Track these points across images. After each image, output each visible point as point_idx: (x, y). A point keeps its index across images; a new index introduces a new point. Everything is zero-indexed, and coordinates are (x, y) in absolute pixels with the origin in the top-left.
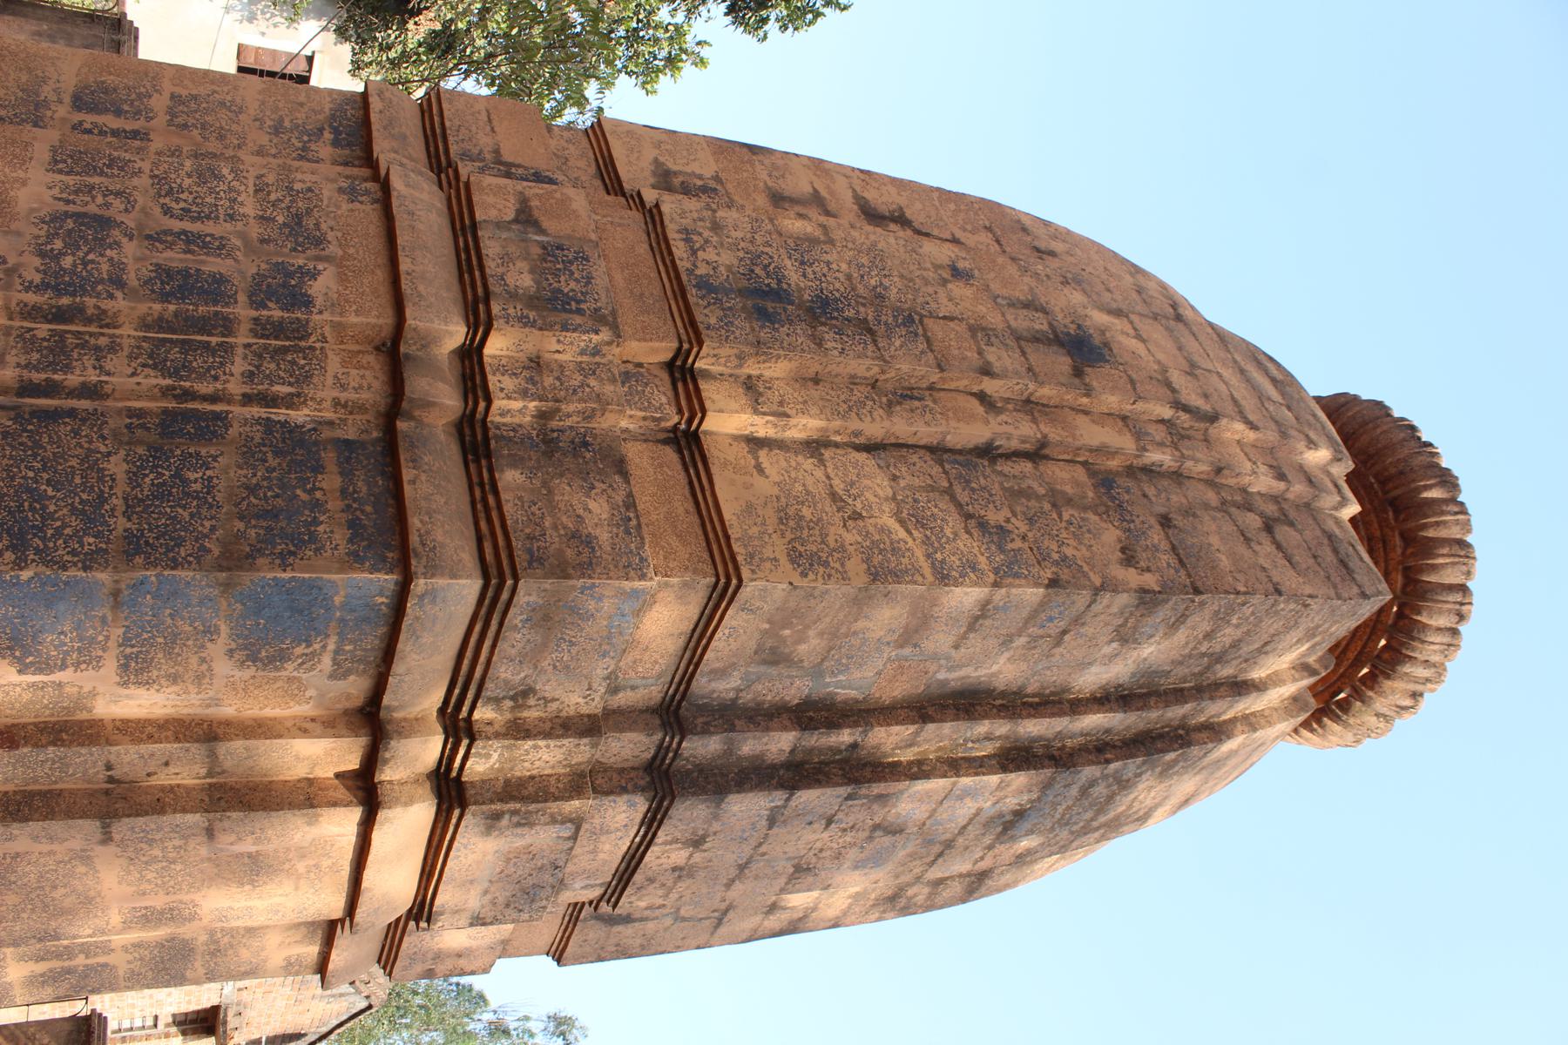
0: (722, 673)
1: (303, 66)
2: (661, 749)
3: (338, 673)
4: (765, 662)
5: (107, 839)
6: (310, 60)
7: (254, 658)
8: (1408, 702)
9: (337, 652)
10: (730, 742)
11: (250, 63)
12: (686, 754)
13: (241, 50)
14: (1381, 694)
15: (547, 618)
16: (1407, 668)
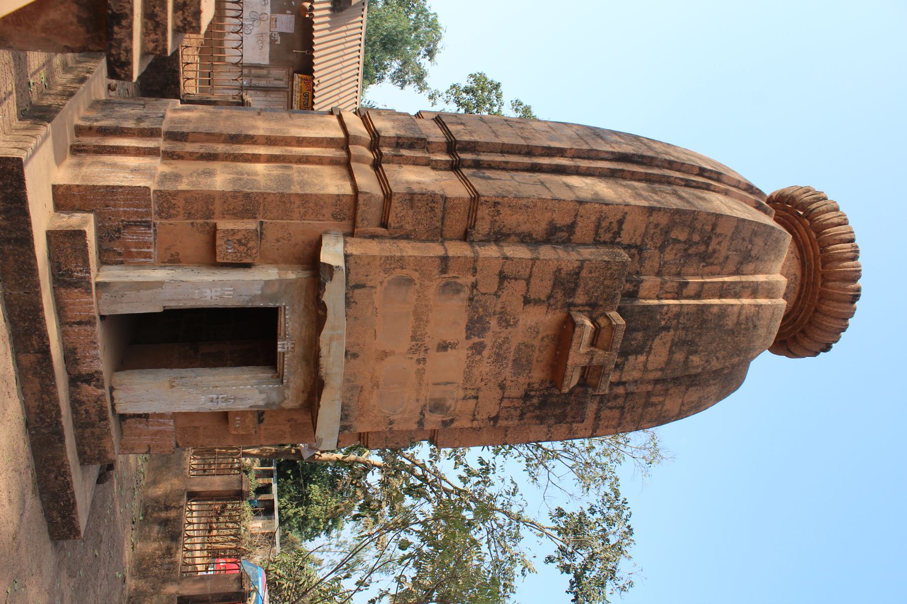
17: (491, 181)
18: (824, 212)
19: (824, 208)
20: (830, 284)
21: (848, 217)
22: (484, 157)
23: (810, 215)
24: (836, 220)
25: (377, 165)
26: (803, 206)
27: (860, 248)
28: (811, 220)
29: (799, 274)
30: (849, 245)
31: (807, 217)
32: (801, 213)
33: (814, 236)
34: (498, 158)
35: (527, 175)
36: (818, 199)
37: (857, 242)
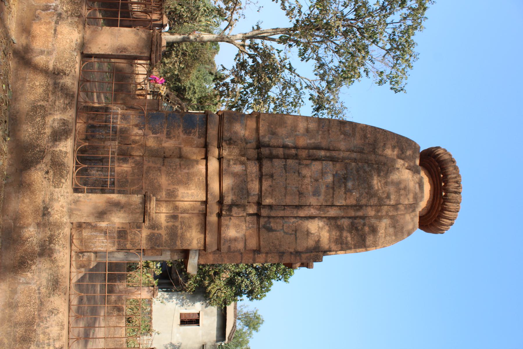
0: (264, 136)
1: (198, 316)
2: (258, 154)
3: (199, 137)
4: (271, 134)
5: (163, 165)
6: (199, 314)
7: (186, 133)
8: (457, 185)
9: (199, 131)
10: (270, 150)
11: (183, 318)
12: (263, 153)
13: (181, 314)
14: (449, 186)
15: (230, 121)
16: (450, 176)
17: (271, 234)
18: (452, 203)
19: (453, 201)
20: (432, 227)
21: (460, 210)
22: (273, 214)
23: (446, 199)
24: (453, 210)
25: (219, 215)
26: (447, 191)
27: (454, 225)
28: (444, 202)
29: (424, 214)
30: (450, 221)
31: (444, 199)
32: (443, 194)
33: (440, 208)
34: (281, 213)
35: (293, 220)
36: (456, 193)
37: (455, 222)
